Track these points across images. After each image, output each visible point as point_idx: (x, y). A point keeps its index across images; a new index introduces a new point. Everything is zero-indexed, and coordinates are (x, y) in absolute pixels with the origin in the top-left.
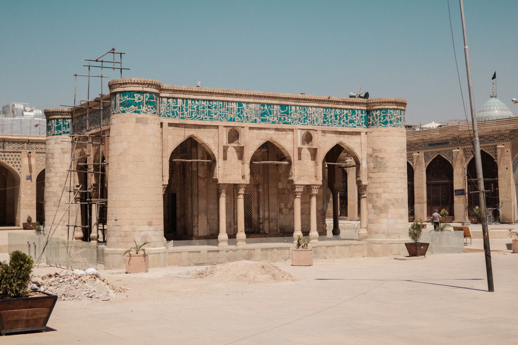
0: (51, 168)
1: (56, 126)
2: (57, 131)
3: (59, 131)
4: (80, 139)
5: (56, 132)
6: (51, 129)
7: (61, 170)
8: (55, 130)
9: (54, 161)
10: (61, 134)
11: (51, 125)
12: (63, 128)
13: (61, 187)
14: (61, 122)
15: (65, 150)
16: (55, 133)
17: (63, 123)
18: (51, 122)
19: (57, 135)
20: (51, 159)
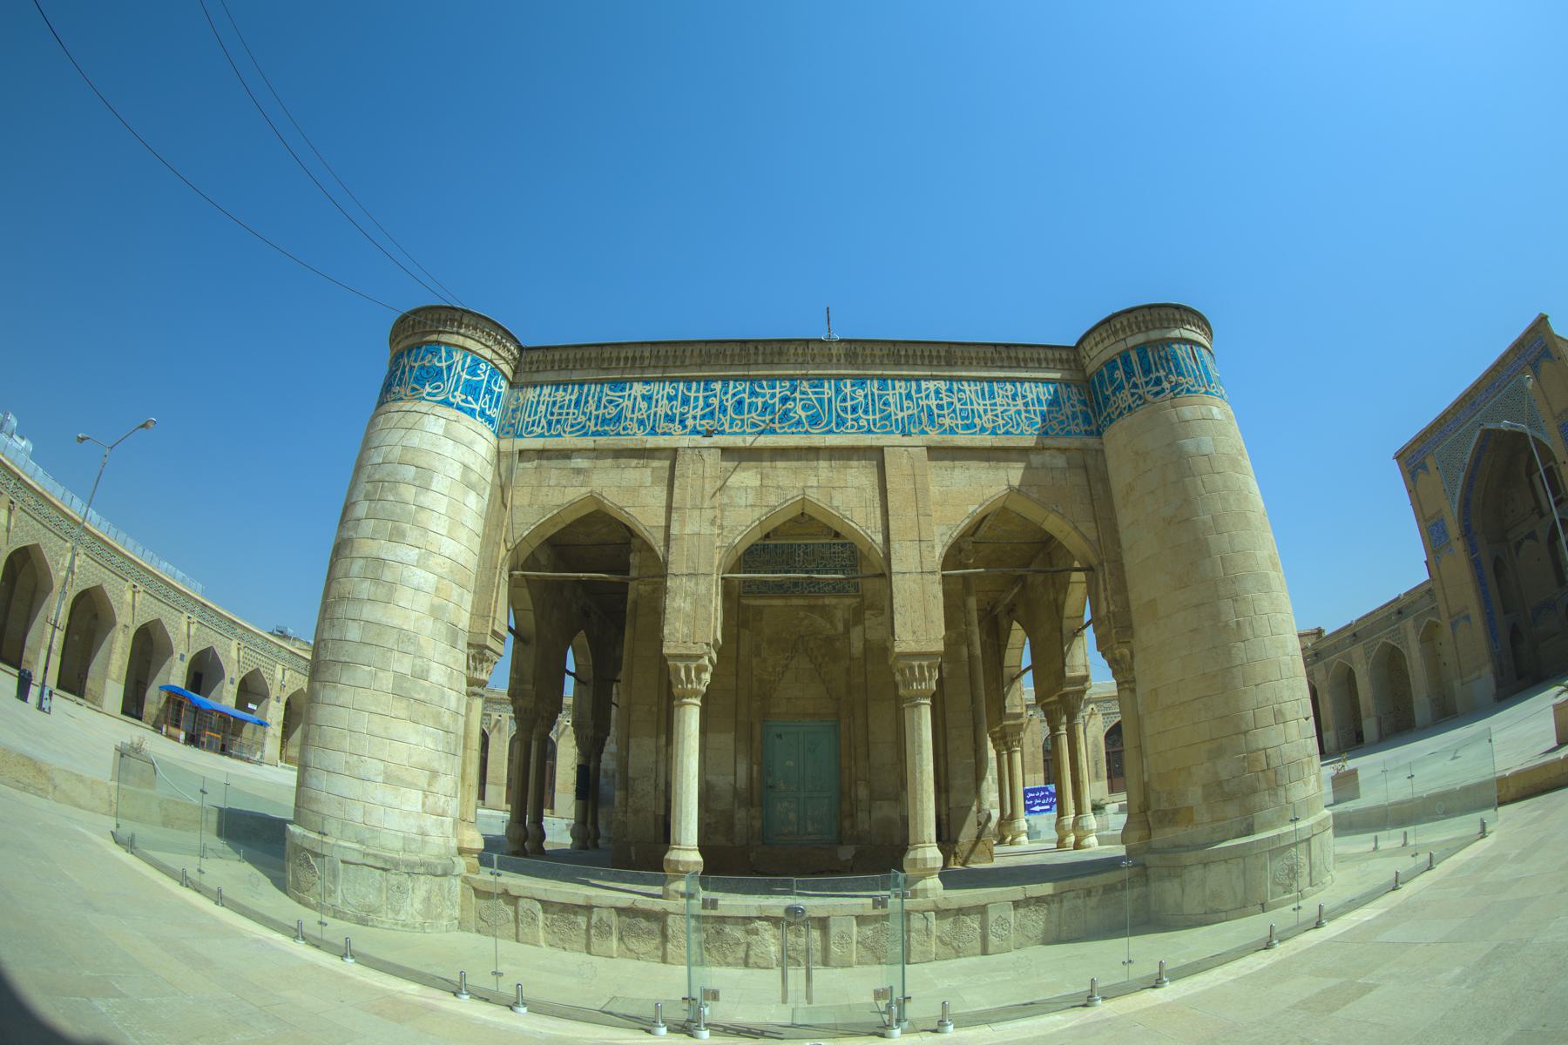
0: (407, 526)
1: (465, 376)
2: (464, 397)
3: (470, 398)
4: (569, 458)
5: (459, 398)
6: (441, 379)
7: (449, 547)
8: (456, 389)
9: (427, 499)
10: (472, 412)
11: (444, 364)
12: (484, 397)
13: (436, 619)
14: (485, 373)
15: (474, 478)
16: (452, 400)
17: (488, 382)
18: (450, 355)
19: (459, 408)
20: (413, 490)
